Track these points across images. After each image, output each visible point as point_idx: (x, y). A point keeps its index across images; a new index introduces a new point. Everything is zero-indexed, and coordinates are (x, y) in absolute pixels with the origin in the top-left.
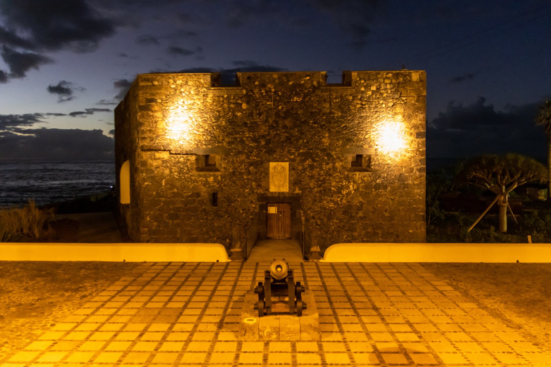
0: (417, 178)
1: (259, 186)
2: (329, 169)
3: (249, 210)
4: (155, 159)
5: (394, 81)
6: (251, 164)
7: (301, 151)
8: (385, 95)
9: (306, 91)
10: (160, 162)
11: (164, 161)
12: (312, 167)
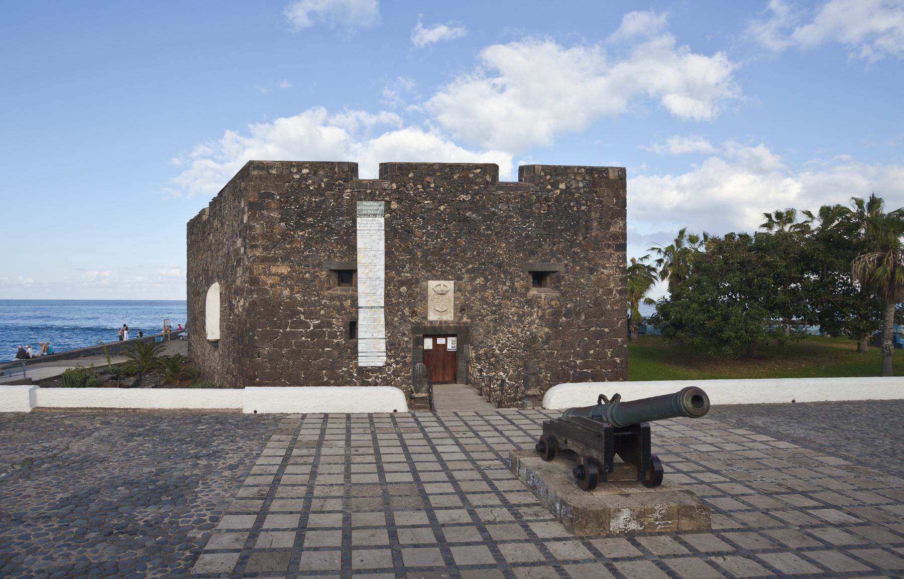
0: (617, 302)
1: (414, 313)
2: (507, 291)
3: (400, 345)
4: (270, 274)
5: (587, 178)
6: (402, 283)
7: (470, 266)
8: (576, 195)
9: (476, 188)
10: (277, 279)
11: (283, 278)
12: (484, 288)
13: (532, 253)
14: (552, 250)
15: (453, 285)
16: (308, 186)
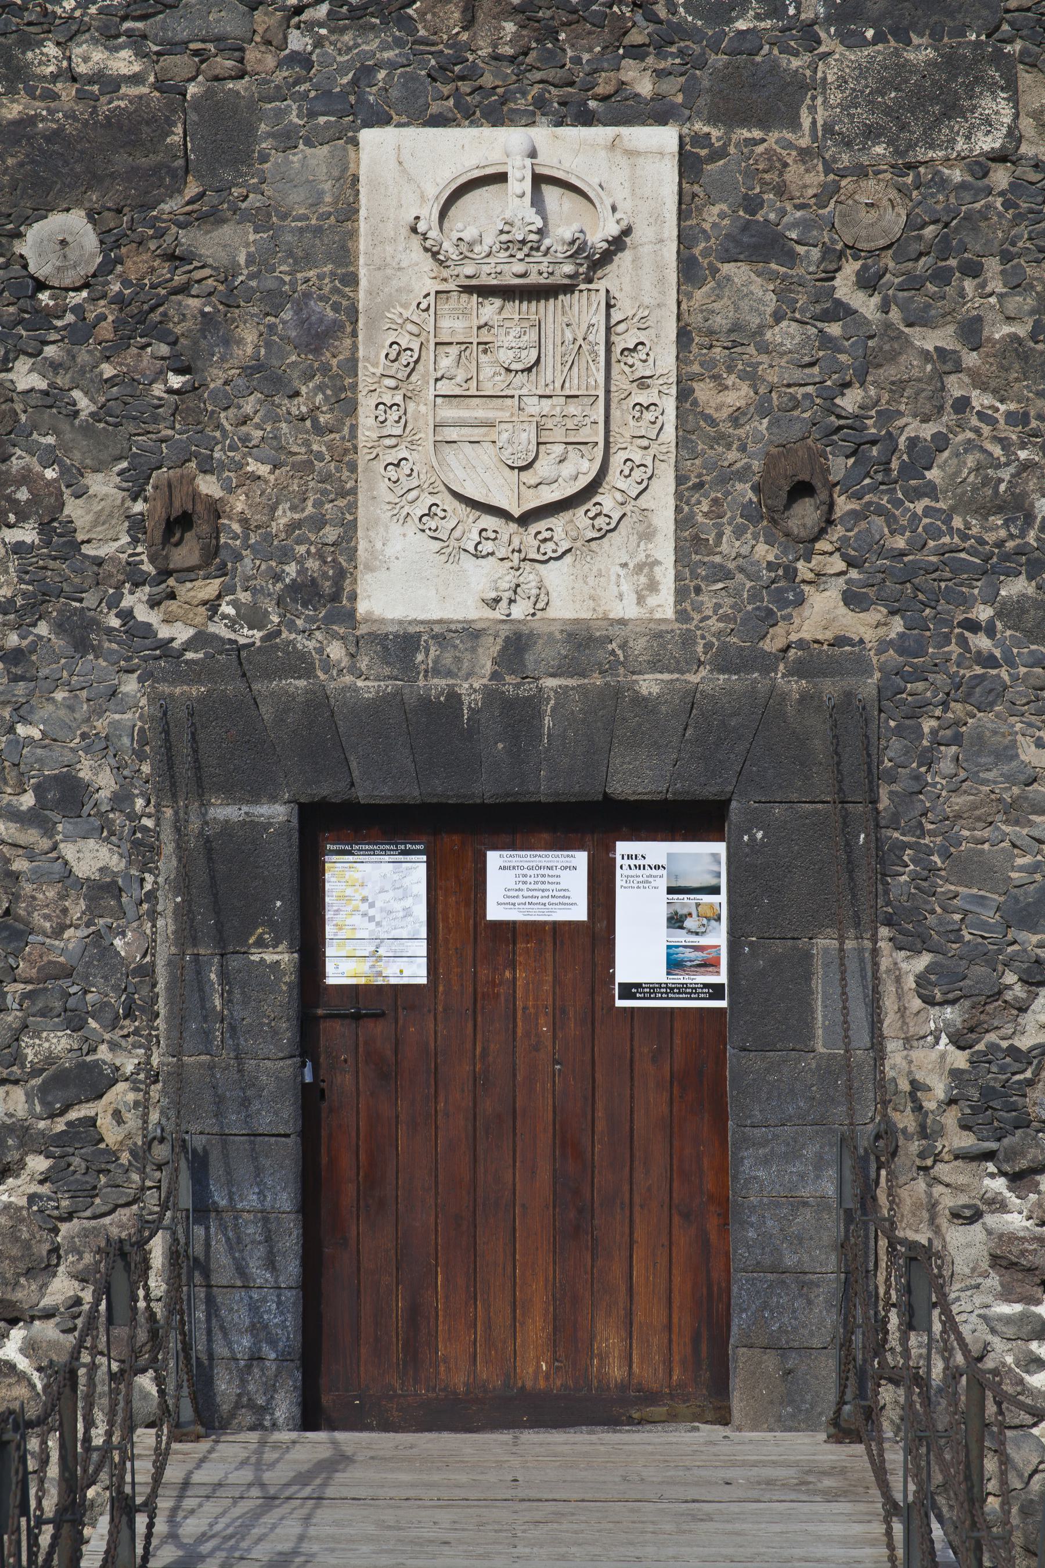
15: (664, 179)
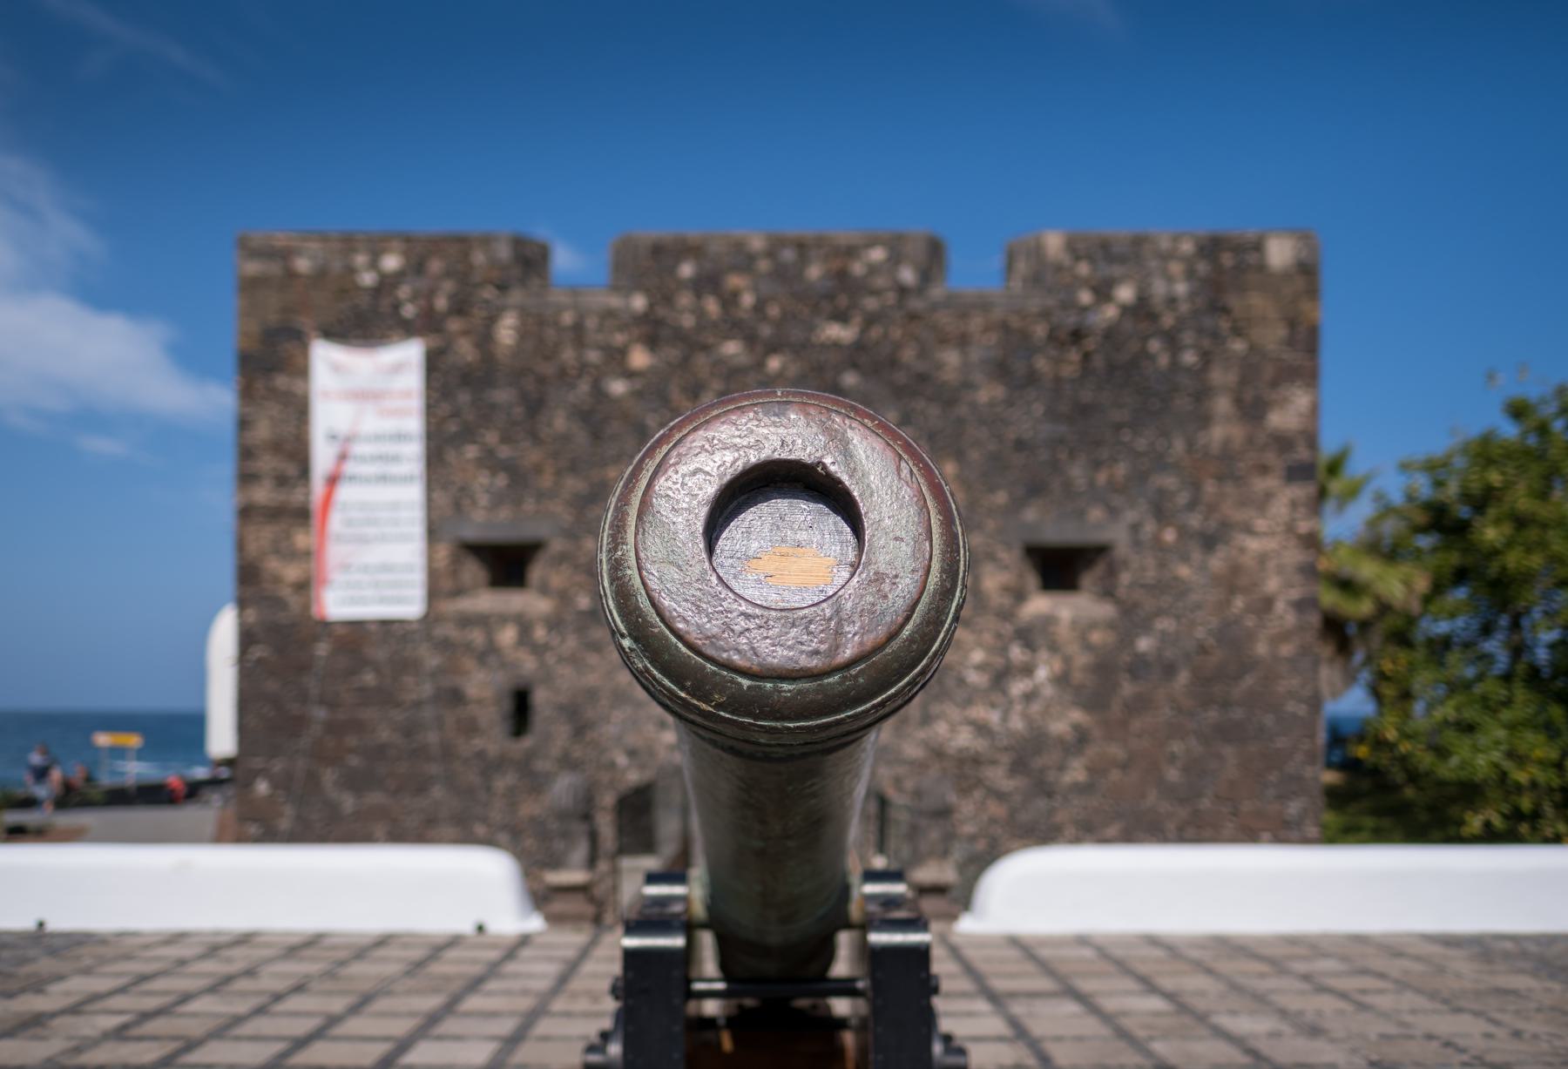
13: (1035, 490)
14: (1091, 484)
16: (396, 306)
